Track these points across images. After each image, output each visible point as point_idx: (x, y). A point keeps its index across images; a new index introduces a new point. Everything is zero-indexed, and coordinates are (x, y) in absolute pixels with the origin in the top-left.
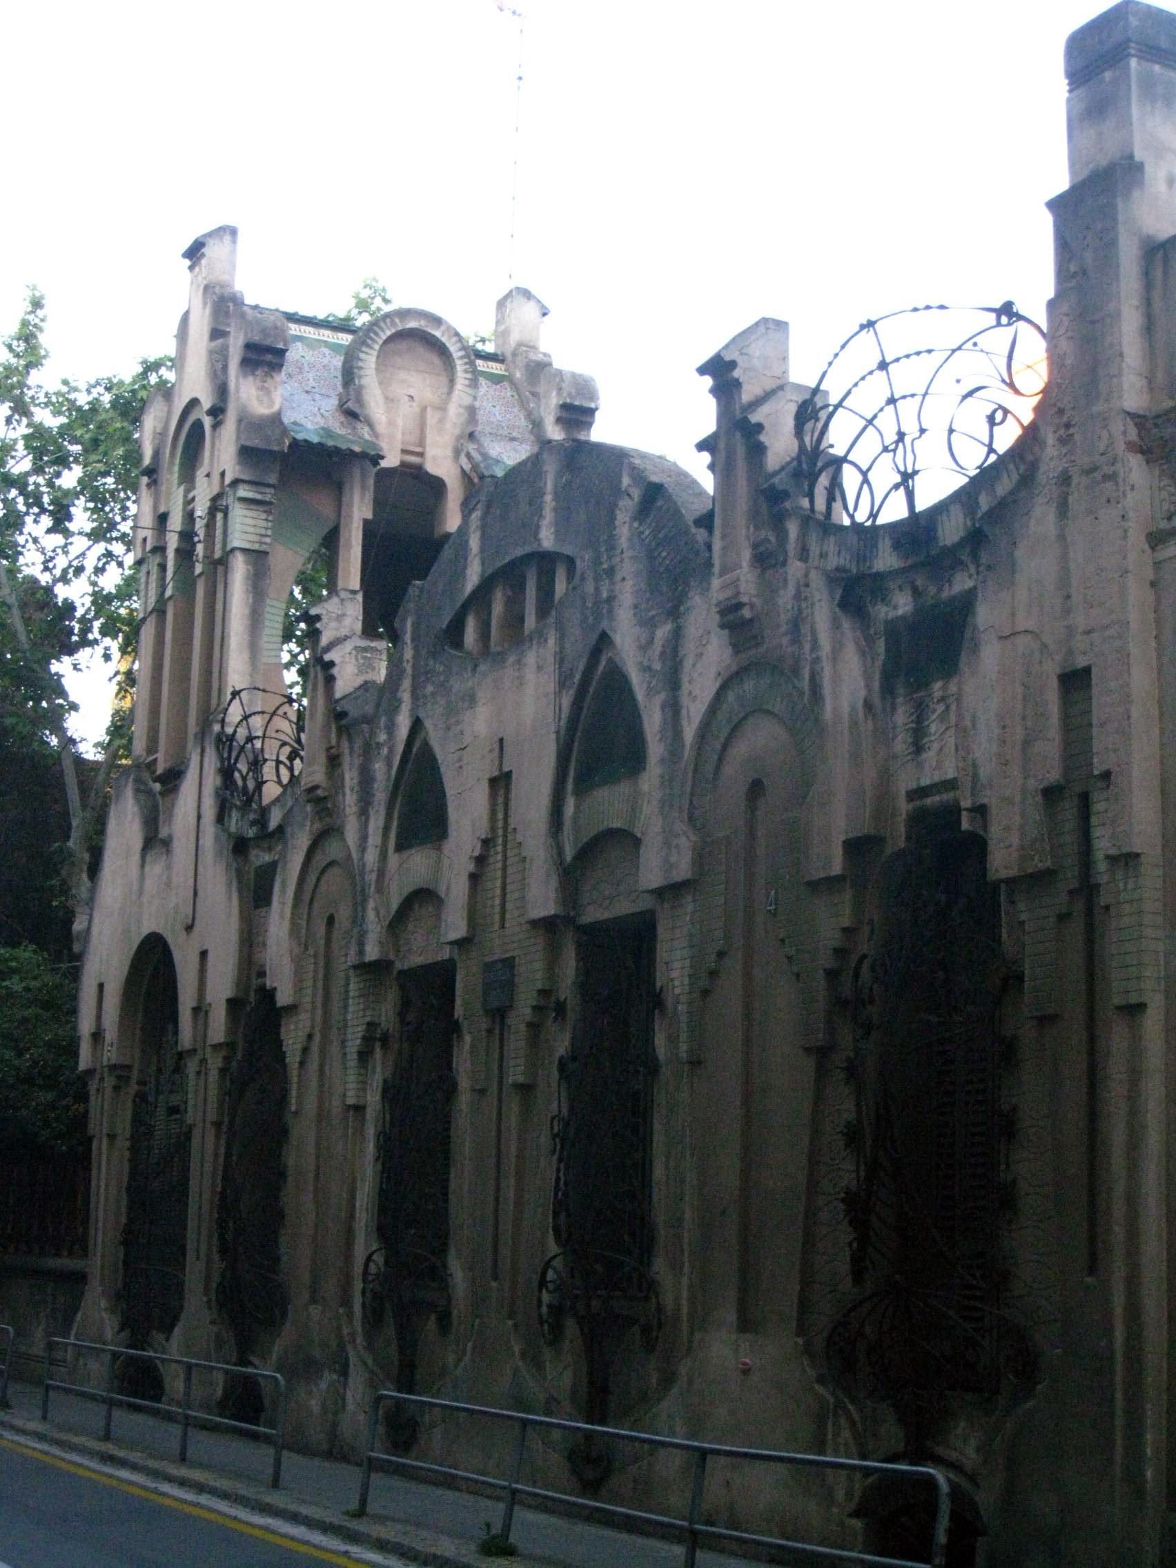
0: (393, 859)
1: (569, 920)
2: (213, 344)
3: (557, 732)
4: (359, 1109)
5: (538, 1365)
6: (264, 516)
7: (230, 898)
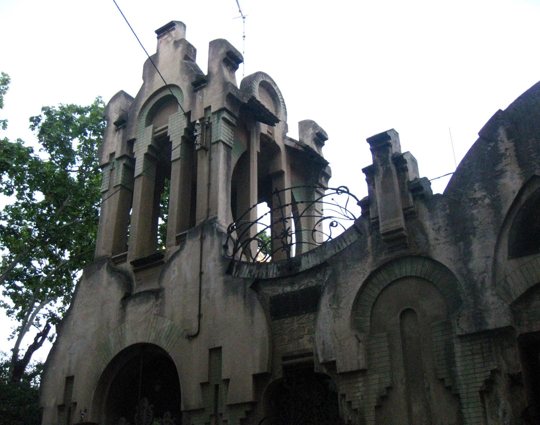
2: (184, 61)
6: (231, 131)
7: (252, 314)
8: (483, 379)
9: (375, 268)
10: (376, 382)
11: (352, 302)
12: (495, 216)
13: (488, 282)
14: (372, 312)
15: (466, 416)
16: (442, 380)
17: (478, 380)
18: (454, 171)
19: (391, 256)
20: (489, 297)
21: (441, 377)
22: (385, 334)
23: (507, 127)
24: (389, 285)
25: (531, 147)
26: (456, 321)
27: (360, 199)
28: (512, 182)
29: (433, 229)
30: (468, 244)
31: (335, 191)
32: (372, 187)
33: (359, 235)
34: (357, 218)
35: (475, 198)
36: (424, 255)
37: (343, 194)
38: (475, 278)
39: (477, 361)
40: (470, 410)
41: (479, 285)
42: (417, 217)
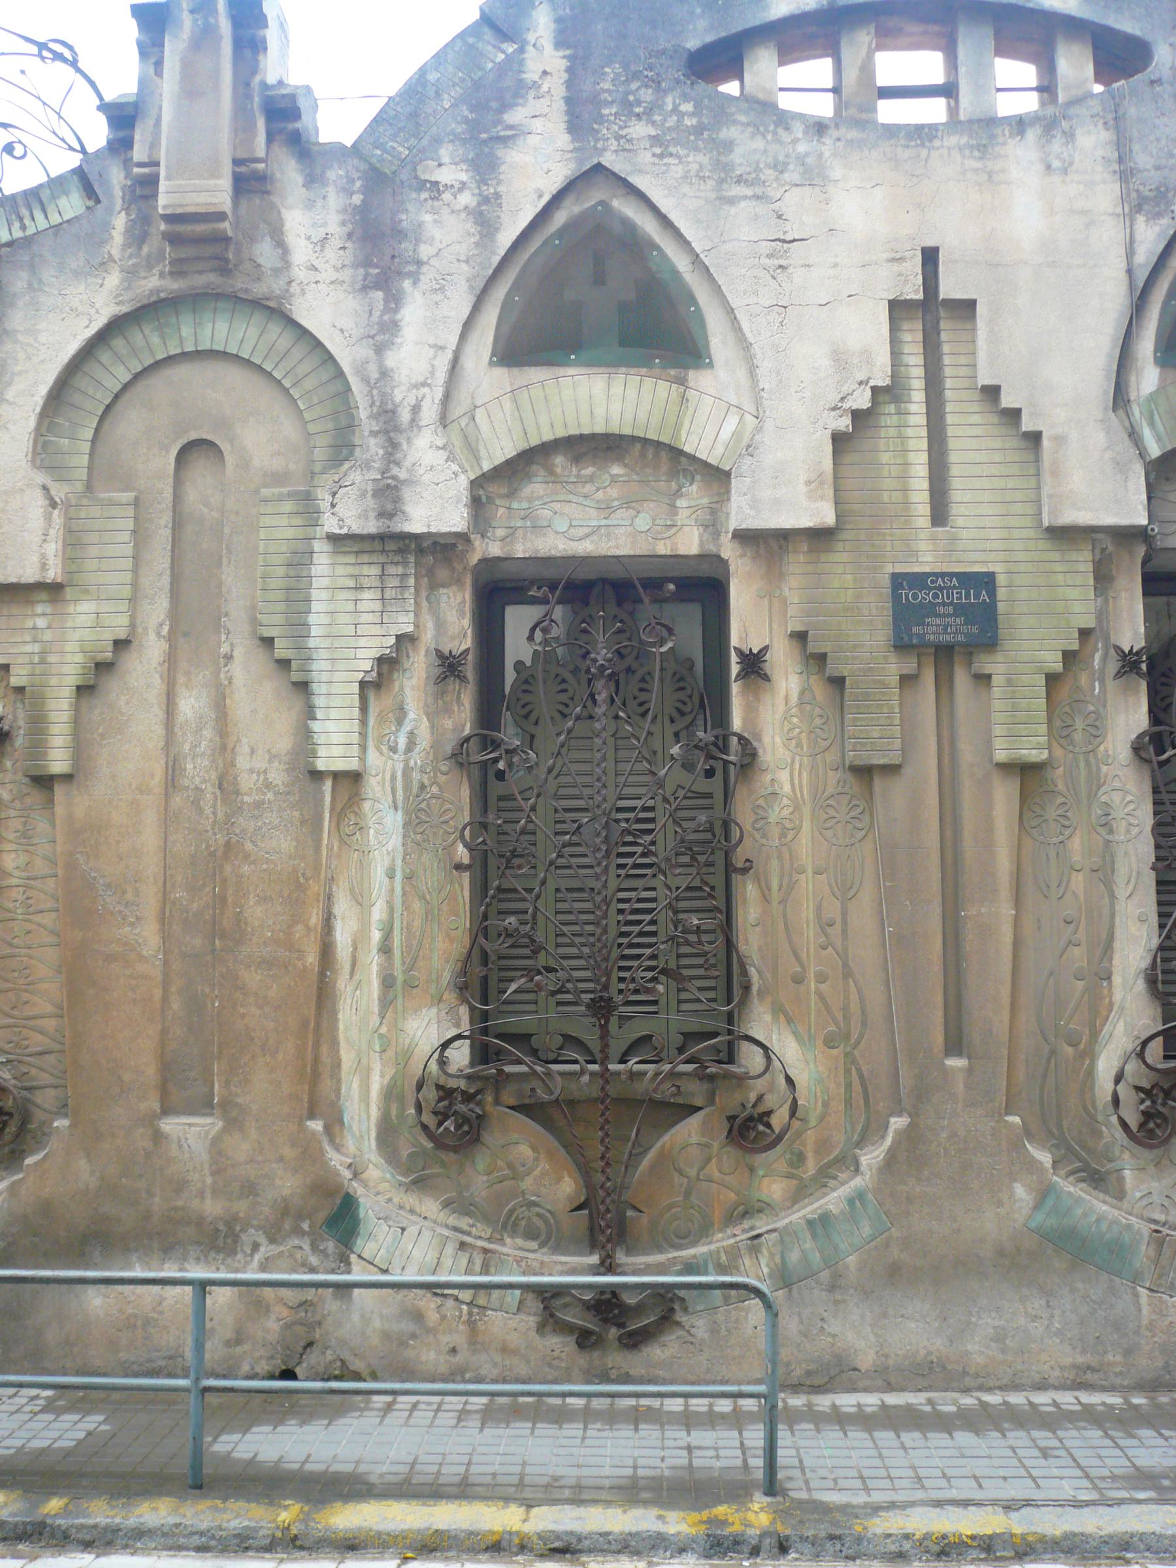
0: (484, 378)
1: (1125, 535)
3: (1129, 271)
4: (351, 780)
5: (1097, 1178)
8: (376, 653)
9: (125, 309)
10: (85, 624)
11: (43, 390)
12: (477, 244)
13: (430, 412)
14: (97, 430)
15: (319, 739)
16: (268, 642)
17: (361, 653)
18: (392, 93)
19: (175, 285)
20: (424, 451)
21: (267, 633)
22: (129, 496)
23: (561, 12)
24: (157, 365)
25: (607, 85)
26: (329, 498)
27: (109, 97)
28: (538, 163)
29: (309, 238)
30: (394, 301)
31: (34, 50)
32: (152, 71)
33: (91, 203)
34: (91, 149)
35: (437, 183)
36: (272, 304)
37: (59, 64)
38: (398, 395)
39: (362, 606)
40: (331, 726)
41: (405, 416)
42: (268, 193)
